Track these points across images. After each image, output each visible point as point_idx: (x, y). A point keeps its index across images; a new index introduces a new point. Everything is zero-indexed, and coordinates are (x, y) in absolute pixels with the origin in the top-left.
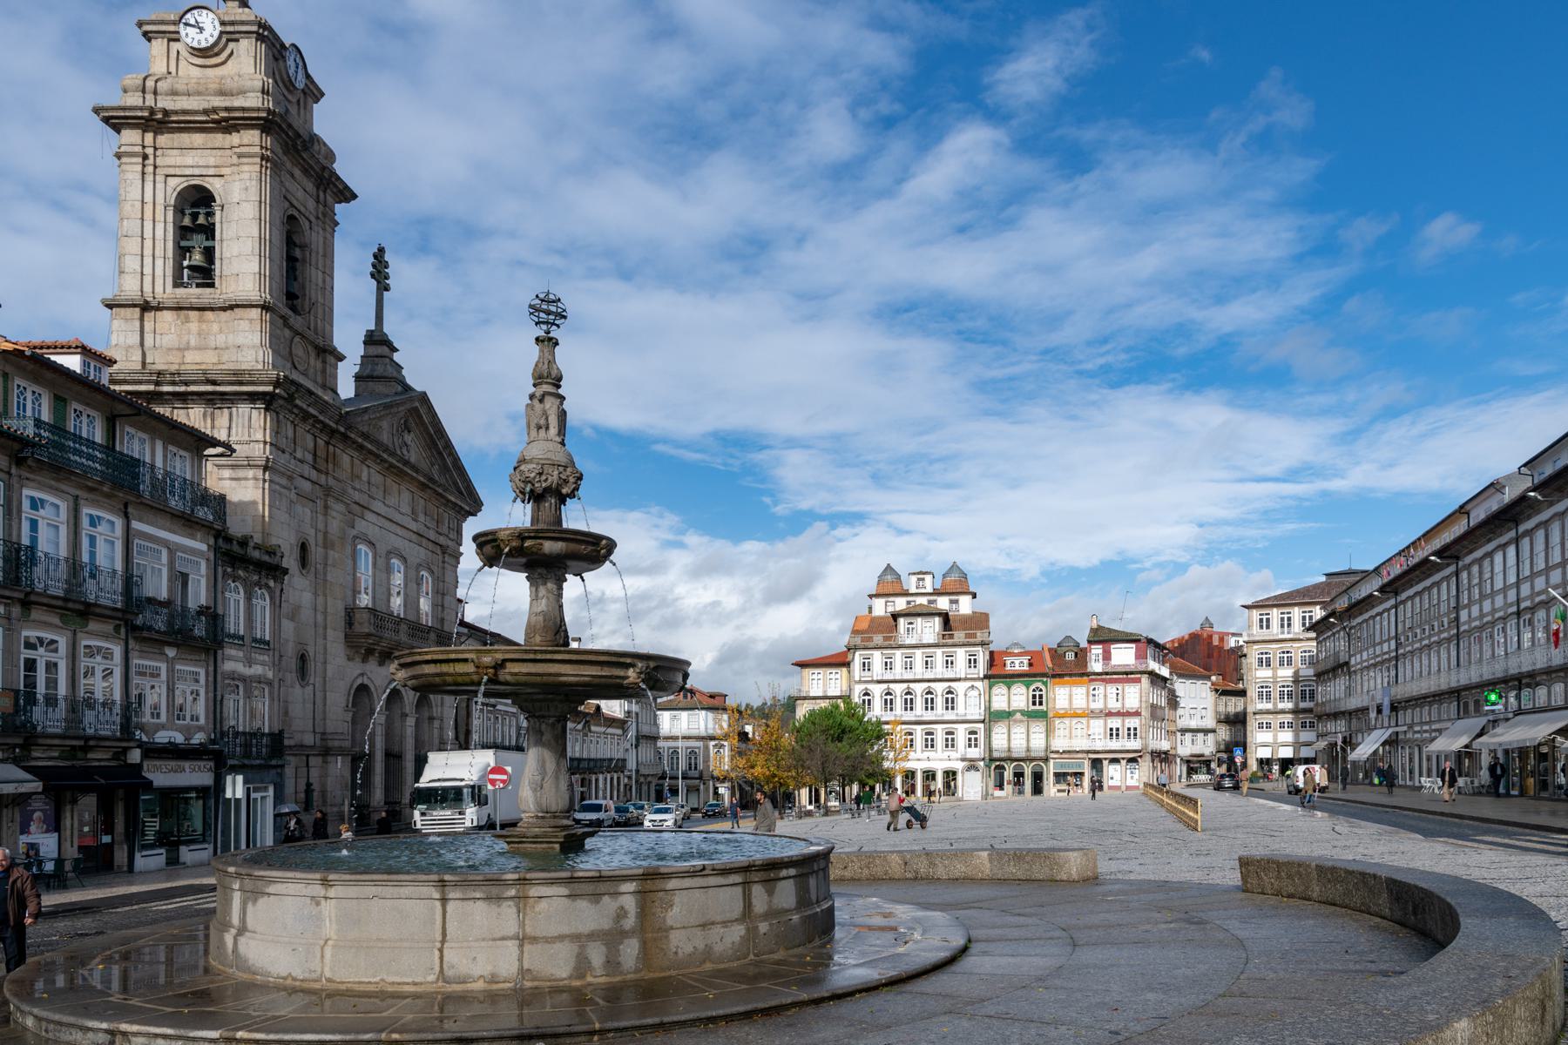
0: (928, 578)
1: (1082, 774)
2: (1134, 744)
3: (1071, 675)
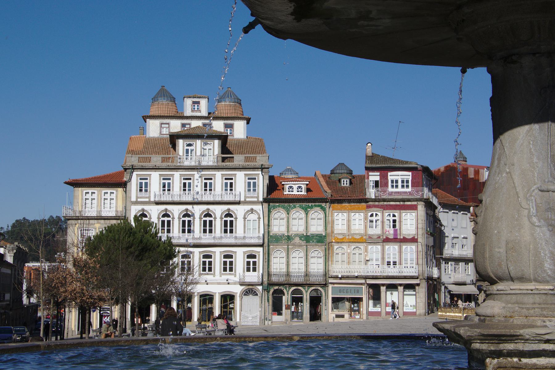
0: (204, 103)
1: (360, 300)
3: (349, 201)
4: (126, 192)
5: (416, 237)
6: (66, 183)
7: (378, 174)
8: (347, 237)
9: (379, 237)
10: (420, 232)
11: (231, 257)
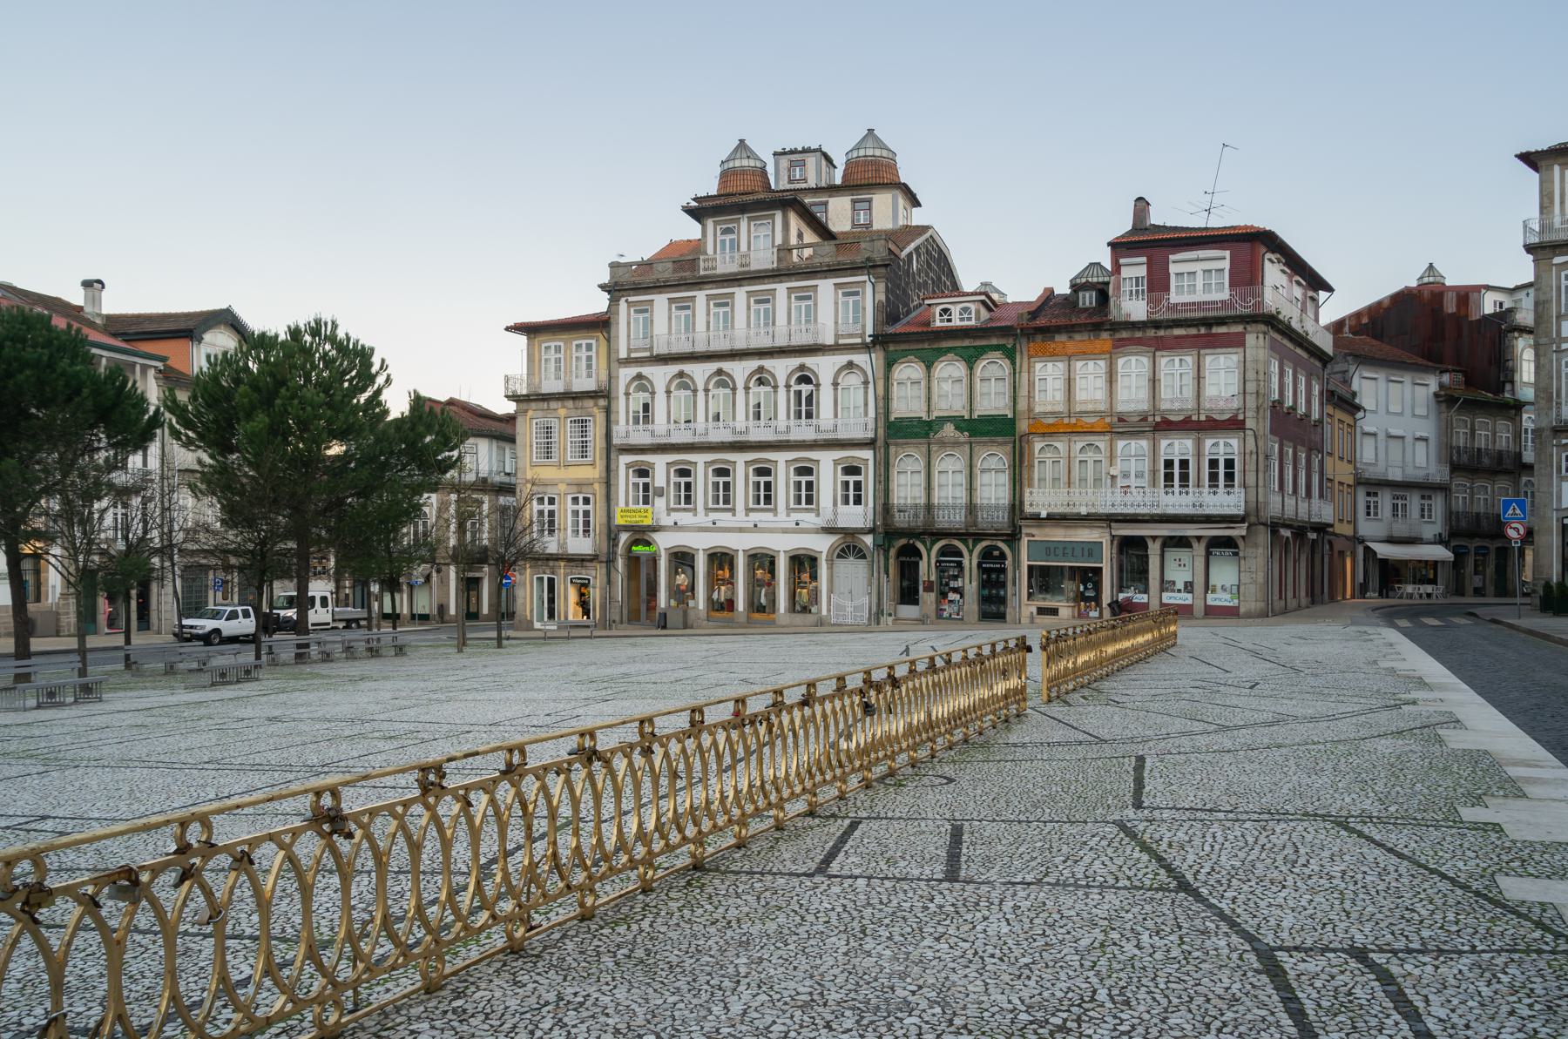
2: (1227, 501)
4: (608, 341)
5: (1241, 417)
6: (507, 329)
7: (1144, 259)
8: (1066, 421)
9: (1145, 419)
10: (1251, 402)
11: (809, 471)
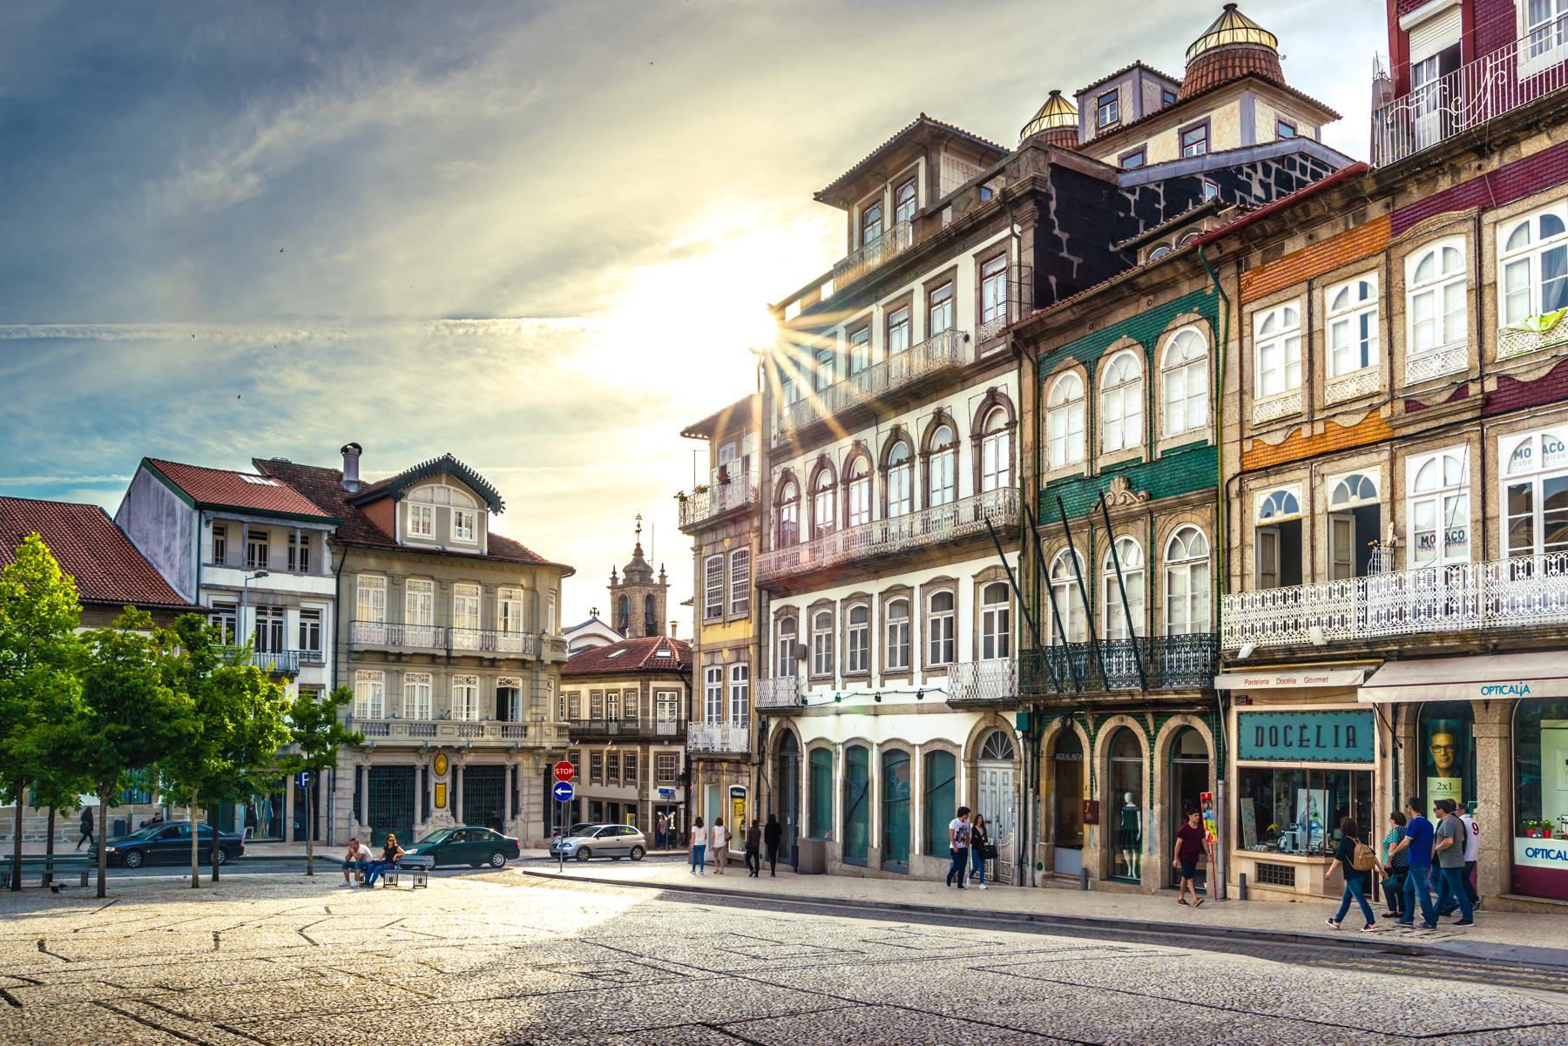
9: (1460, 392)
